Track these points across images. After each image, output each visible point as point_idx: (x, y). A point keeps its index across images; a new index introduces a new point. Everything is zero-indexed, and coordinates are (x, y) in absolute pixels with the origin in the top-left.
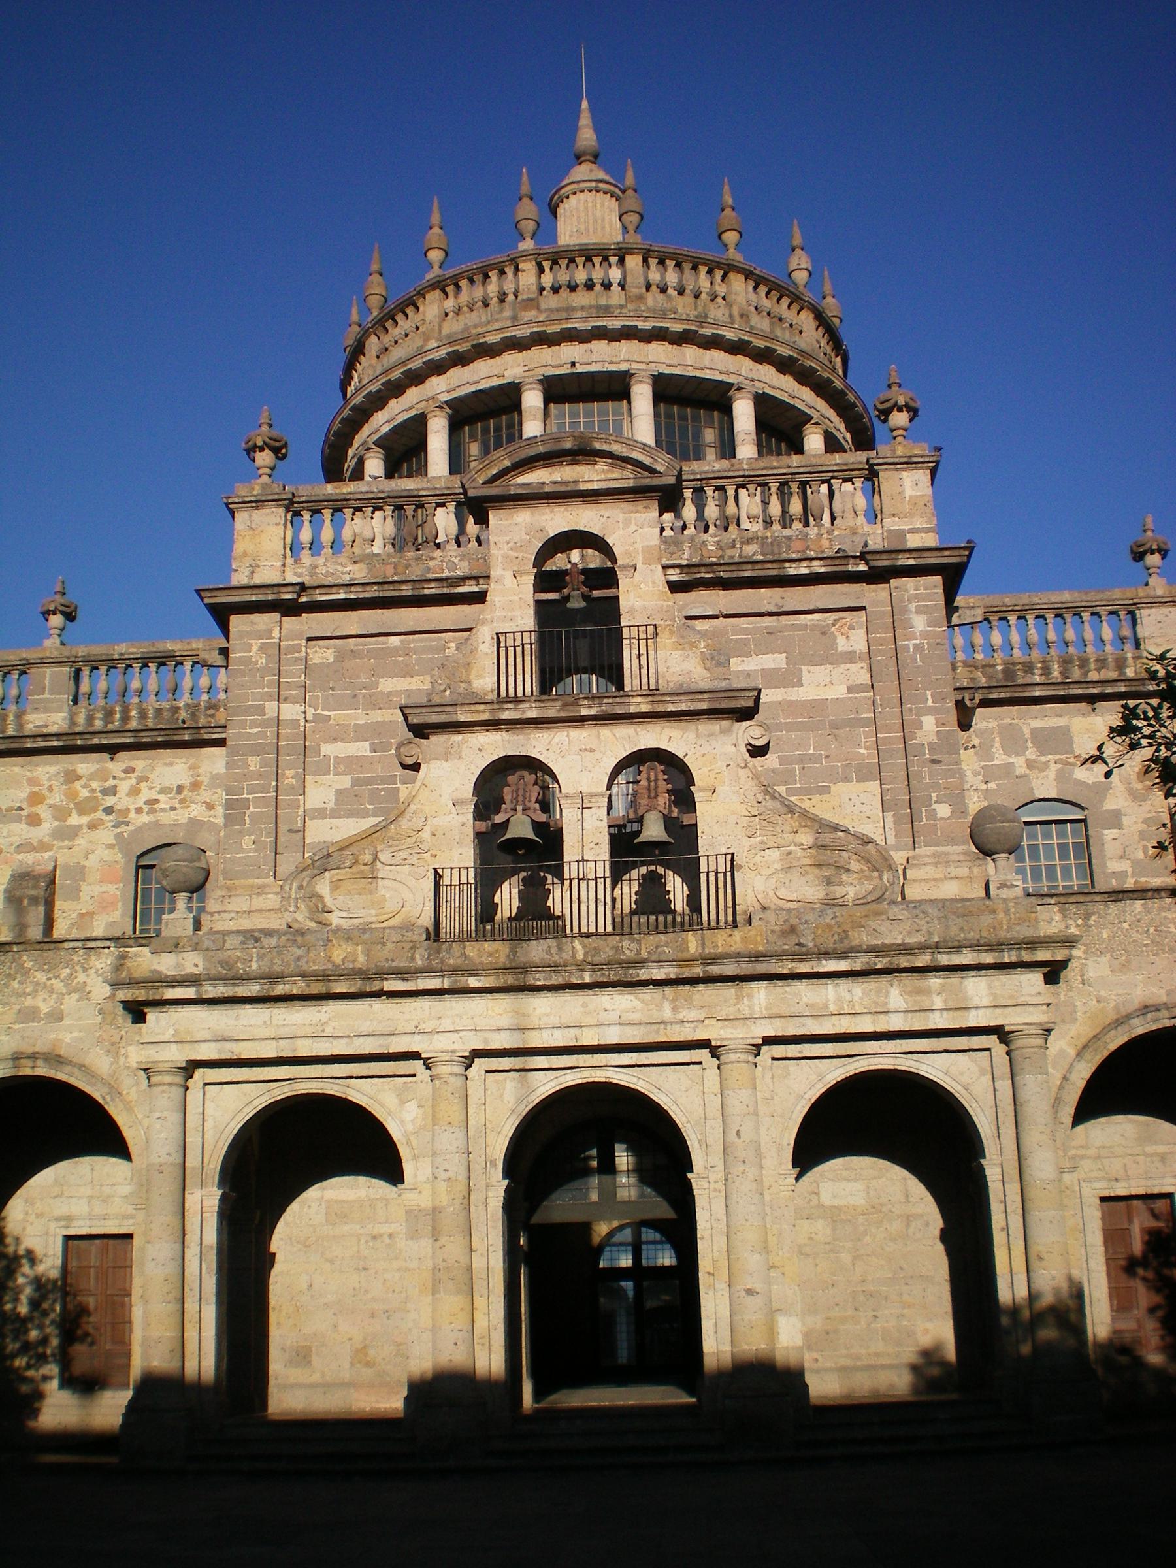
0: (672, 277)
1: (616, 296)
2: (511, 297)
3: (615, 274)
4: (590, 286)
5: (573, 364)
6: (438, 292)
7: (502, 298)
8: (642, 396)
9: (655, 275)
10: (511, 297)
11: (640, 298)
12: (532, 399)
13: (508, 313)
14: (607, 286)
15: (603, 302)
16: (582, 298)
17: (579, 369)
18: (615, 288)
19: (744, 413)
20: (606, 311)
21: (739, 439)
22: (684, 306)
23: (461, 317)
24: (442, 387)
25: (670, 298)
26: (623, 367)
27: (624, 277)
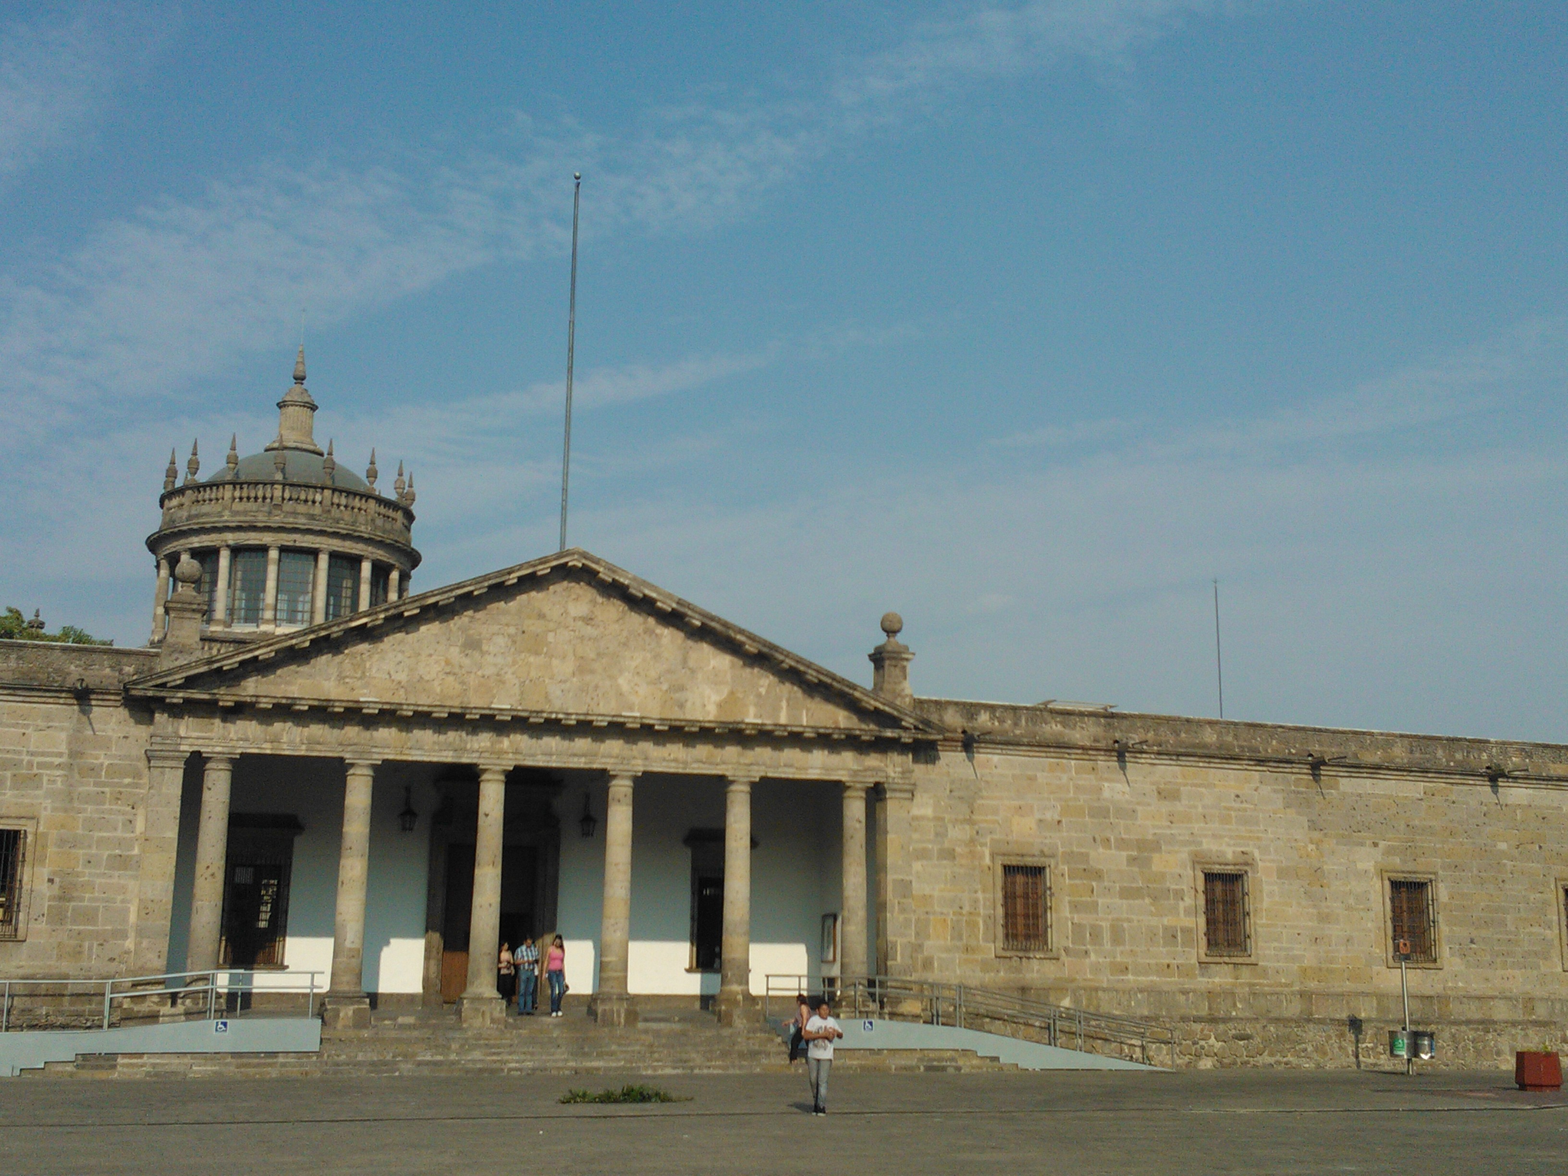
0: (343, 501)
1: (317, 510)
2: (268, 500)
3: (318, 497)
4: (306, 501)
5: (295, 541)
6: (231, 486)
7: (264, 498)
8: (323, 561)
9: (336, 500)
10: (268, 500)
11: (329, 511)
12: (273, 554)
13: (266, 509)
14: (314, 502)
15: (311, 512)
16: (301, 508)
17: (297, 544)
18: (317, 504)
19: (366, 568)
20: (312, 517)
21: (363, 580)
22: (347, 515)
23: (243, 503)
24: (231, 538)
25: (341, 511)
26: (317, 546)
27: (323, 498)
